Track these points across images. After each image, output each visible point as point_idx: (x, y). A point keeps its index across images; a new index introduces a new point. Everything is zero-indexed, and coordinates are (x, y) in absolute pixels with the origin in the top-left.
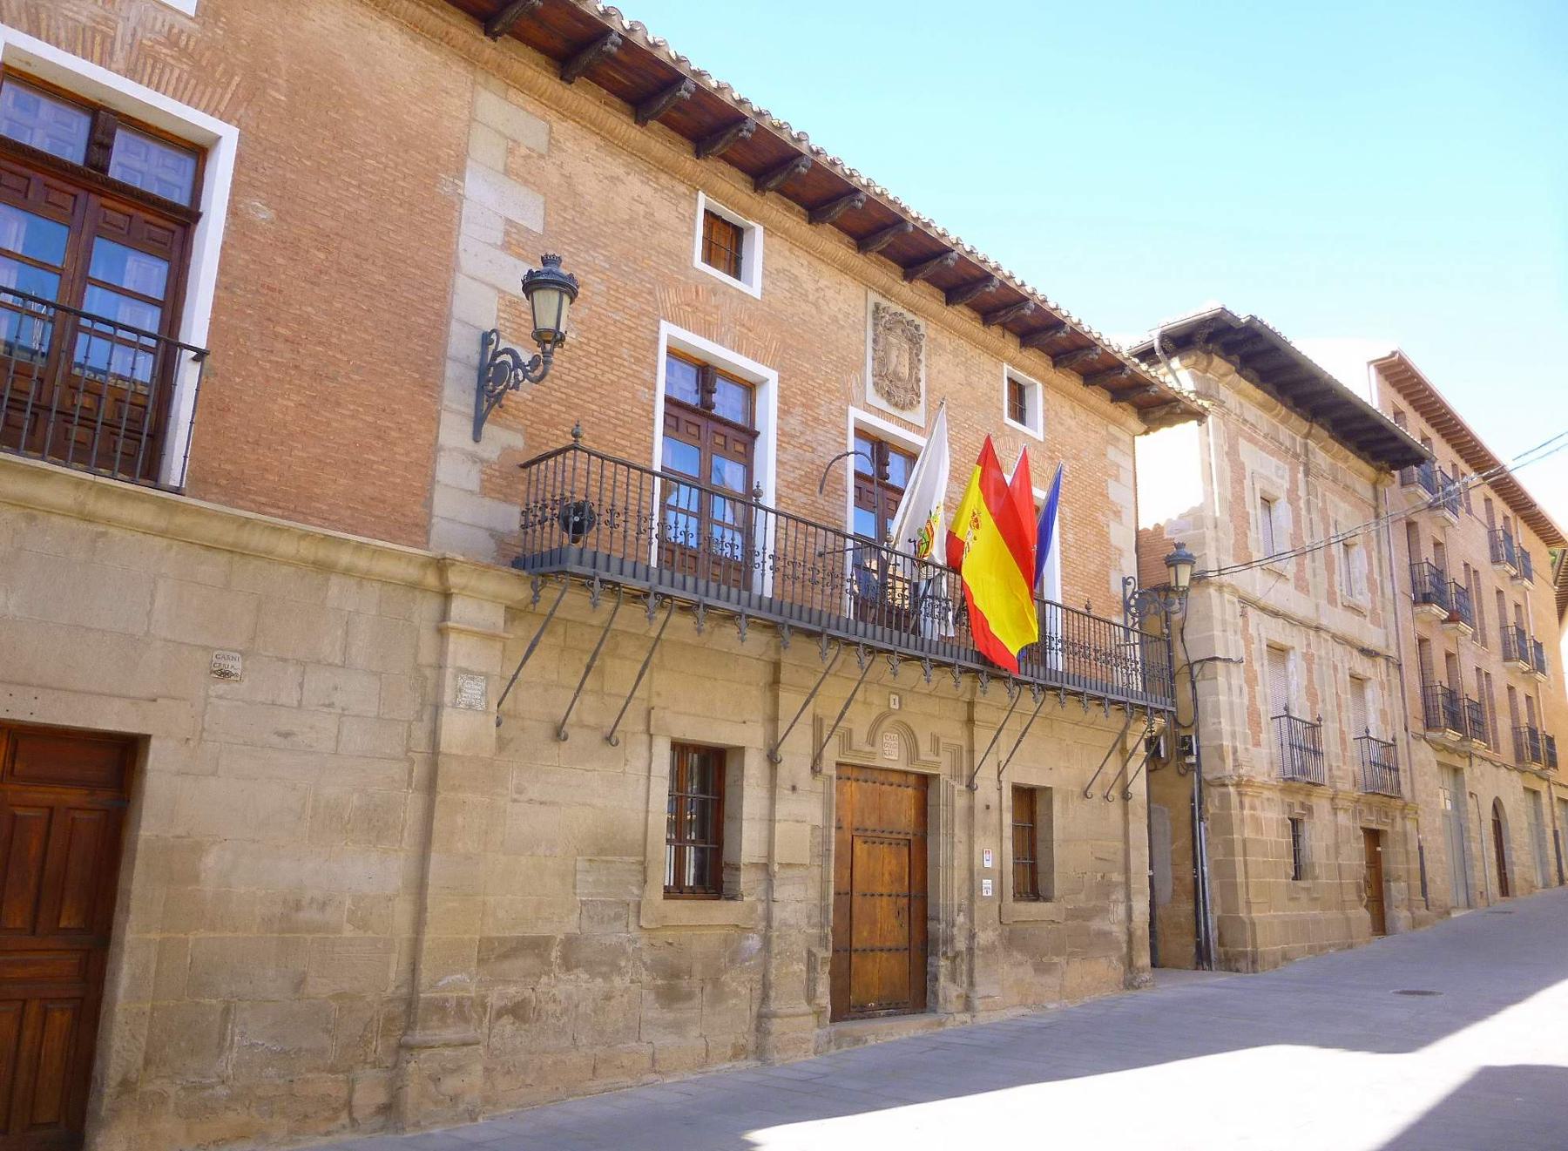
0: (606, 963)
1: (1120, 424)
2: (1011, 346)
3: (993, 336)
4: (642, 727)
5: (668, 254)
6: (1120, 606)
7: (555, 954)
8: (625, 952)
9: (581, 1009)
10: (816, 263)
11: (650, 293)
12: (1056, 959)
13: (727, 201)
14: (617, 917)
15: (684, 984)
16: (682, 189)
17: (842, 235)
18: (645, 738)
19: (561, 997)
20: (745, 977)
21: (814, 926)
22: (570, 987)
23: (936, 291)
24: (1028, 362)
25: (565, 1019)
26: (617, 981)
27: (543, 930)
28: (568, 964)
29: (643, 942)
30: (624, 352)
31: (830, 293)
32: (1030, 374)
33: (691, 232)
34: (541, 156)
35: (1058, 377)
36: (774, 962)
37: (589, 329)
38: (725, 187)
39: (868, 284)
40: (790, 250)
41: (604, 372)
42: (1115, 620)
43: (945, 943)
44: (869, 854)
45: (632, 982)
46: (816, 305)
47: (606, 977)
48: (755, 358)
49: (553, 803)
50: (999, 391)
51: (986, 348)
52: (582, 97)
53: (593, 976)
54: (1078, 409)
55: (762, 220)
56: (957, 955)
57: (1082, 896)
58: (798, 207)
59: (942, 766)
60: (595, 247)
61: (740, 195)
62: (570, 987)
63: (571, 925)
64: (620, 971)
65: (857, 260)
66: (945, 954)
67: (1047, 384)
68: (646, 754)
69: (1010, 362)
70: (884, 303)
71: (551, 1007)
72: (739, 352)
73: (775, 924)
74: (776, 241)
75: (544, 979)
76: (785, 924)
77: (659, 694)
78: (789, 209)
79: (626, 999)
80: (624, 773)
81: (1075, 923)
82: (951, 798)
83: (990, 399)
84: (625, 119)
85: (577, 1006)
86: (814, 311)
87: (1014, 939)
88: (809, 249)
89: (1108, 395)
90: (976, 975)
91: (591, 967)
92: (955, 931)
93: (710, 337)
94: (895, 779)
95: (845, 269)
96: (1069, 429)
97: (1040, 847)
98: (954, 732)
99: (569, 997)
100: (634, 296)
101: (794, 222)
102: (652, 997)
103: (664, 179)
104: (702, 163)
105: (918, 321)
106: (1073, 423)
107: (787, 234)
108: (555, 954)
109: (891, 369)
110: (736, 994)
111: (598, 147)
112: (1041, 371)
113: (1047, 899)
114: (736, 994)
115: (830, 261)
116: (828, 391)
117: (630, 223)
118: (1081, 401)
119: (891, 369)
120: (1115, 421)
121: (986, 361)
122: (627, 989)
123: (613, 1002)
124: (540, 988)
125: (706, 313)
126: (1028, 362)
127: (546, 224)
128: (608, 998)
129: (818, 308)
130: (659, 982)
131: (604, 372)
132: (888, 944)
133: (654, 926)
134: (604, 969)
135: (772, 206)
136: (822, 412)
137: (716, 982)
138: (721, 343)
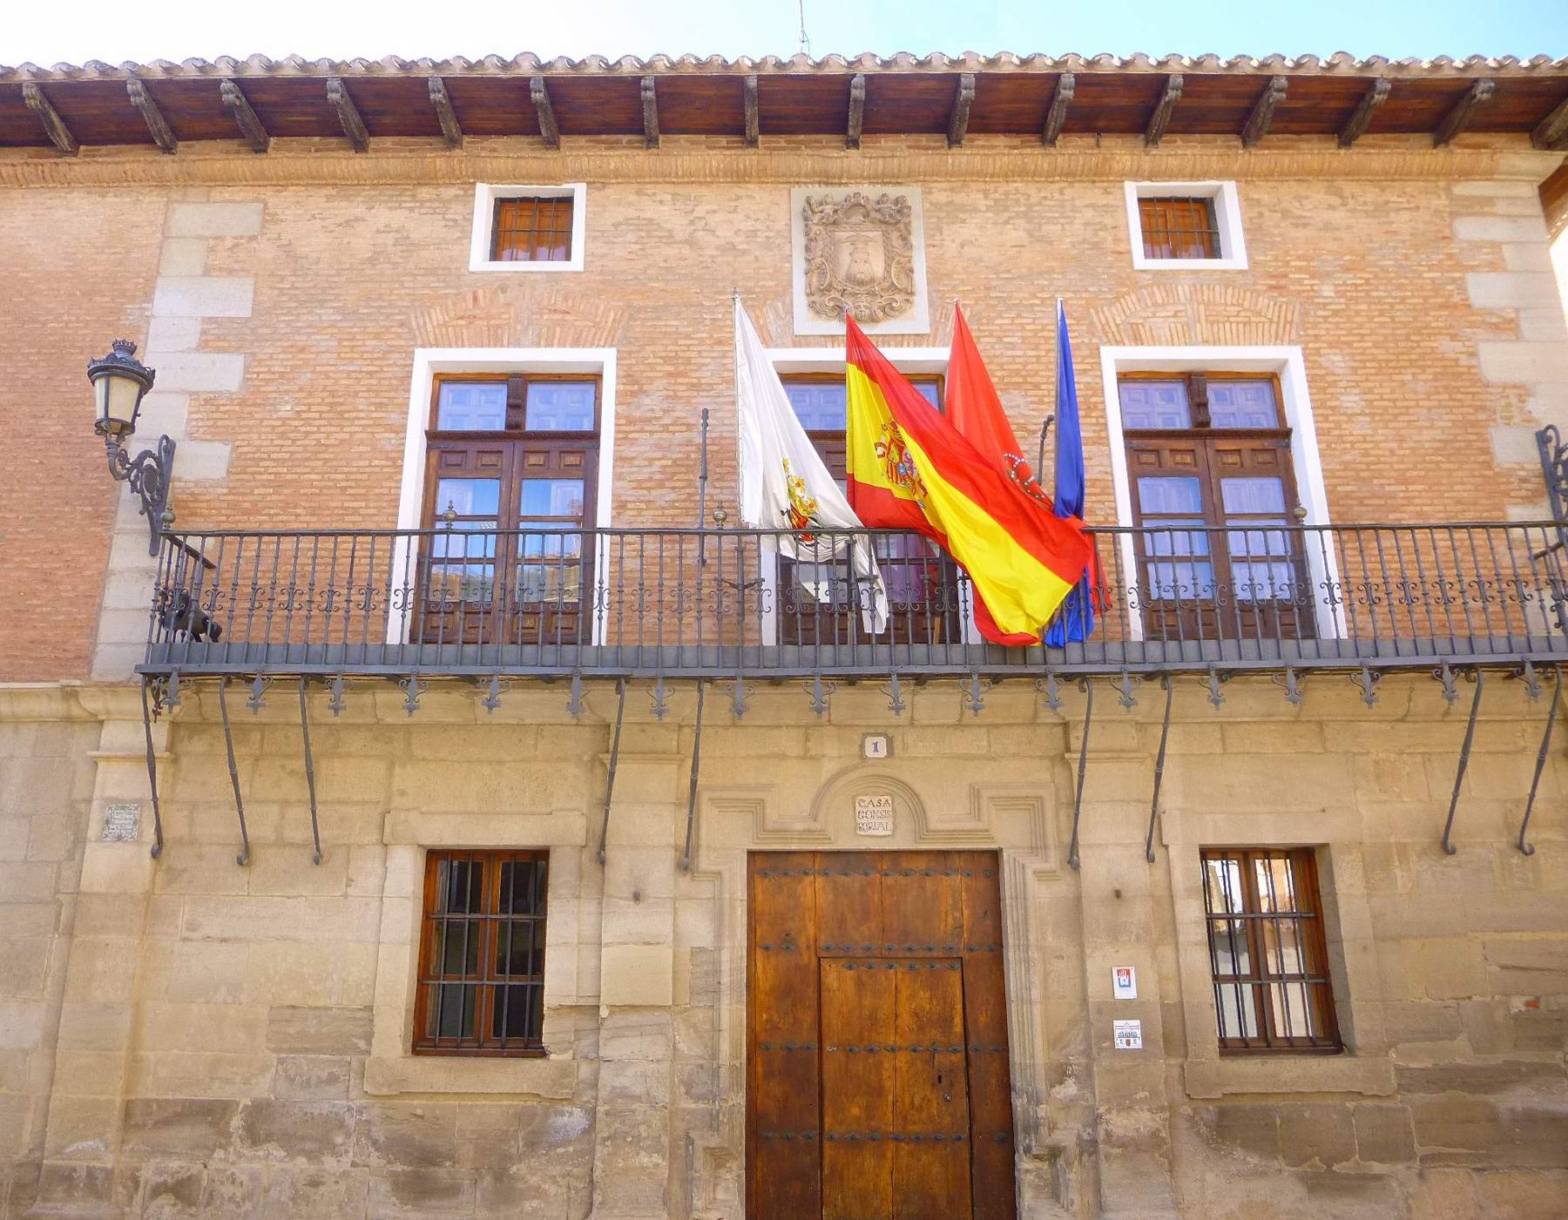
0: (317, 1137)
1: (1489, 175)
2: (1121, 152)
3: (1075, 151)
4: (375, 837)
5: (431, 272)
6: (1537, 483)
7: (236, 1122)
8: (341, 1125)
9: (274, 1193)
10: (681, 190)
11: (402, 325)
12: (1377, 1168)
13: (517, 178)
14: (332, 1079)
15: (442, 1173)
16: (453, 191)
17: (713, 138)
18: (378, 849)
19: (244, 1178)
20: (556, 1170)
21: (698, 1098)
22: (256, 1166)
23: (924, 139)
24: (1173, 162)
25: (248, 1206)
26: (329, 1162)
27: (217, 1093)
28: (254, 1137)
29: (375, 1113)
30: (361, 403)
31: (714, 220)
32: (1193, 176)
33: (466, 234)
34: (253, 238)
35: (1260, 158)
36: (600, 1151)
37: (310, 394)
38: (501, 164)
39: (790, 179)
40: (639, 193)
41: (329, 434)
42: (1516, 513)
43: (1027, 1131)
44: (860, 984)
45: (354, 1164)
46: (691, 242)
47: (312, 1156)
48: (576, 343)
49: (237, 940)
50: (1120, 228)
51: (1070, 175)
52: (284, 157)
53: (292, 1153)
54: (1349, 188)
55: (577, 177)
56: (1054, 1153)
57: (1462, 1041)
58: (625, 138)
59: (1005, 832)
60: (322, 303)
61: (522, 163)
62: (256, 1166)
63: (262, 1088)
64: (333, 1149)
65: (748, 159)
66: (1028, 1150)
67: (1244, 177)
68: (380, 871)
69: (1136, 175)
70: (817, 192)
71: (227, 1190)
72: (549, 344)
73: (603, 1094)
74: (612, 192)
75: (219, 1153)
76: (624, 1094)
77: (403, 793)
78: (611, 146)
79: (342, 1186)
80: (346, 896)
81: (1439, 1097)
82: (1032, 891)
83: (1096, 246)
84: (341, 154)
85: (266, 1191)
86: (686, 251)
87: (1234, 1127)
88: (664, 178)
89: (1427, 139)
90: (1105, 1190)
91: (290, 1142)
92: (1042, 1111)
93: (498, 343)
94: (922, 864)
95: (740, 177)
96: (1328, 227)
97: (1330, 949)
98: (1038, 776)
99: (254, 1177)
100: (377, 336)
101: (623, 156)
102: (385, 1187)
103: (424, 193)
104: (457, 152)
105: (893, 192)
106: (1339, 216)
107: (620, 176)
108: (236, 1122)
109: (842, 273)
110: (538, 1193)
111: (329, 198)
112: (1215, 163)
113: (1352, 1053)
114: (538, 1193)
115: (710, 179)
116: (719, 342)
117: (372, 261)
118: (1350, 174)
119: (842, 273)
120: (1467, 175)
121: (1084, 195)
122: (345, 1174)
123: (322, 1189)
124: (213, 1165)
125: (489, 317)
126: (1173, 162)
127: (256, 304)
128: (315, 1183)
129: (691, 242)
130: (399, 1167)
131: (329, 434)
132: (915, 1129)
133: (385, 1091)
134: (309, 1146)
135: (579, 153)
136: (706, 375)
137: (501, 1176)
138: (517, 344)
